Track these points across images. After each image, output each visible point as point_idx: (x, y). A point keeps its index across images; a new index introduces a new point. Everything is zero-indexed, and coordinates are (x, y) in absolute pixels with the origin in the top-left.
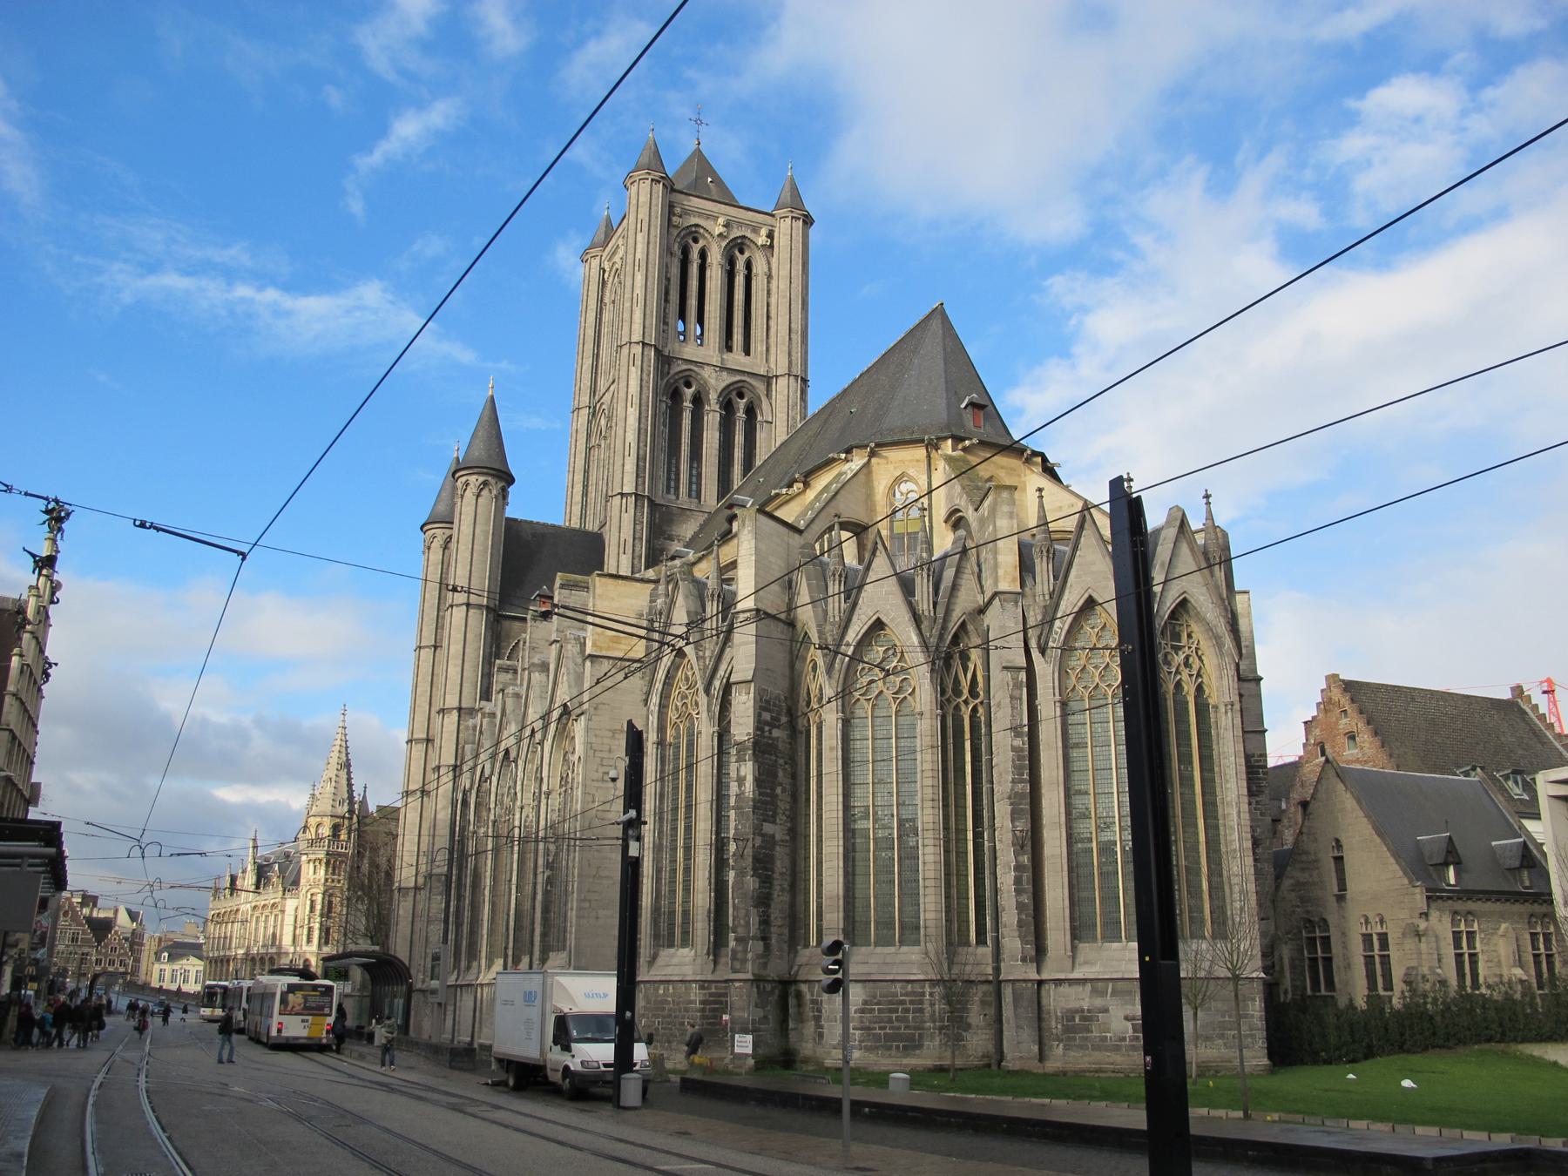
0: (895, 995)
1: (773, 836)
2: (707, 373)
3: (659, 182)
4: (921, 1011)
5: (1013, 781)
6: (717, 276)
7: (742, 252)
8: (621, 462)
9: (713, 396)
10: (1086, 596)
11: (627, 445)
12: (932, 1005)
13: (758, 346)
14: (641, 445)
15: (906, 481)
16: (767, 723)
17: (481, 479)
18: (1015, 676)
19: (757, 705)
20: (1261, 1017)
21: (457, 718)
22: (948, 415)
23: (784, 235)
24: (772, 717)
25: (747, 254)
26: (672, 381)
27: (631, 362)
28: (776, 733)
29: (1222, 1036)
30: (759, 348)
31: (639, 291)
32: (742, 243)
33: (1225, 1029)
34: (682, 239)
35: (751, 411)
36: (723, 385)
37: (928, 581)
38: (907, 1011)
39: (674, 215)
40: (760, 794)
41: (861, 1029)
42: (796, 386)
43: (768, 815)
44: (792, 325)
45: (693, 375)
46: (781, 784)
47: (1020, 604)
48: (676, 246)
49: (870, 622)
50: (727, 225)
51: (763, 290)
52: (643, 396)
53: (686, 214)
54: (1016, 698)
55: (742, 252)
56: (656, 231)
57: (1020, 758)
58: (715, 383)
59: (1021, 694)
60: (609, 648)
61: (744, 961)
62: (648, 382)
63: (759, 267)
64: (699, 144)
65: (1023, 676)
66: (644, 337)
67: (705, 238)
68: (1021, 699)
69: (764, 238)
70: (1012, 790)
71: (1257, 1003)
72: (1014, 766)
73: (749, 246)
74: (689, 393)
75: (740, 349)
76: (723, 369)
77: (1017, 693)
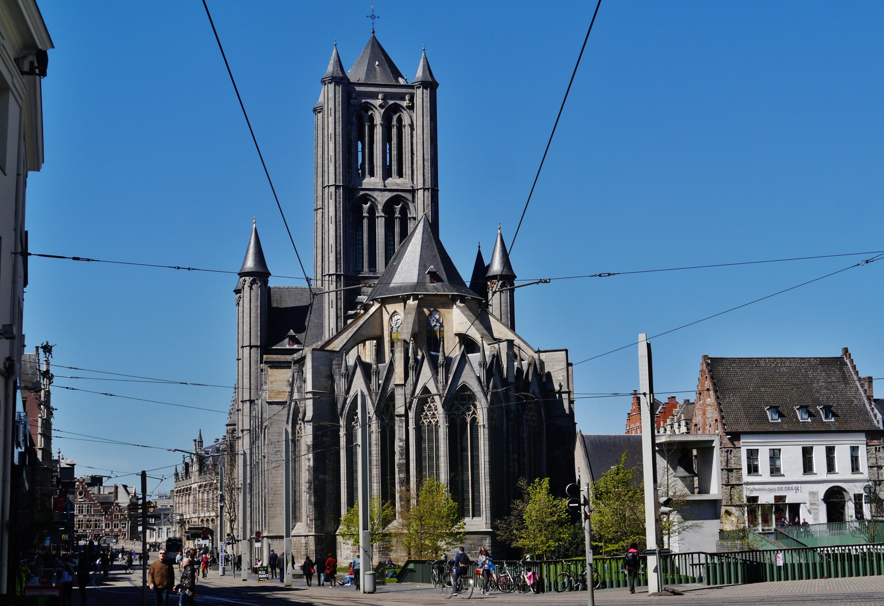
1: (324, 480)
2: (375, 194)
5: (399, 459)
6: (379, 132)
7: (395, 113)
8: (327, 256)
9: (380, 207)
11: (330, 246)
13: (407, 170)
14: (338, 245)
15: (397, 315)
20: (489, 546)
21: (249, 405)
22: (418, 281)
23: (419, 98)
27: (330, 198)
28: (324, 439)
30: (407, 173)
31: (332, 153)
33: (471, 550)
35: (404, 211)
36: (386, 199)
37: (376, 377)
39: (352, 99)
41: (353, 552)
42: (428, 194)
44: (425, 157)
48: (354, 118)
51: (408, 135)
52: (338, 216)
54: (401, 427)
56: (339, 114)
57: (402, 450)
60: (275, 398)
61: (312, 528)
62: (340, 208)
63: (406, 121)
64: (374, 32)
65: (403, 418)
67: (372, 109)
68: (402, 427)
69: (408, 101)
72: (400, 454)
74: (366, 207)
75: (396, 174)
77: (401, 425)
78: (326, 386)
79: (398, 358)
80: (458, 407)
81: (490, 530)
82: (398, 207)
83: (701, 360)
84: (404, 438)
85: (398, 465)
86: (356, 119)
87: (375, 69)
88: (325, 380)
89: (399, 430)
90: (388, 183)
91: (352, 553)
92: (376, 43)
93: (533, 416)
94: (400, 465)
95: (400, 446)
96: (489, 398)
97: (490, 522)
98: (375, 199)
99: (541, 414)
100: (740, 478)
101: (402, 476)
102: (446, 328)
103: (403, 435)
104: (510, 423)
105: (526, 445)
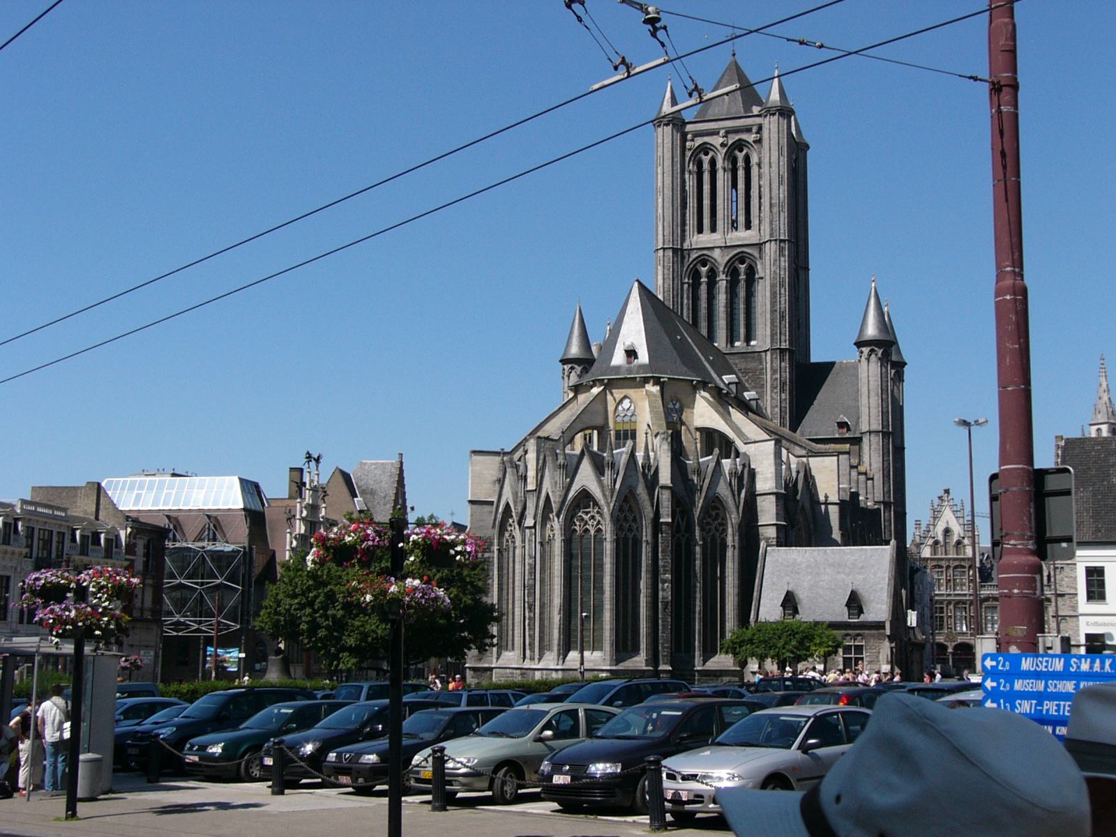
2: (716, 254)
7: (741, 151)
13: (755, 221)
17: (570, 366)
25: (744, 152)
26: (691, 266)
28: (486, 555)
35: (751, 271)
44: (773, 201)
45: (706, 257)
50: (725, 136)
58: (720, 258)
63: (754, 159)
64: (734, 55)
65: (533, 530)
66: (664, 244)
76: (726, 247)
81: (608, 668)
82: (742, 267)
83: (1053, 443)
86: (693, 164)
90: (731, 239)
92: (734, 67)
95: (529, 564)
96: (612, 505)
97: (609, 658)
98: (716, 260)
100: (1075, 608)
102: (639, 419)
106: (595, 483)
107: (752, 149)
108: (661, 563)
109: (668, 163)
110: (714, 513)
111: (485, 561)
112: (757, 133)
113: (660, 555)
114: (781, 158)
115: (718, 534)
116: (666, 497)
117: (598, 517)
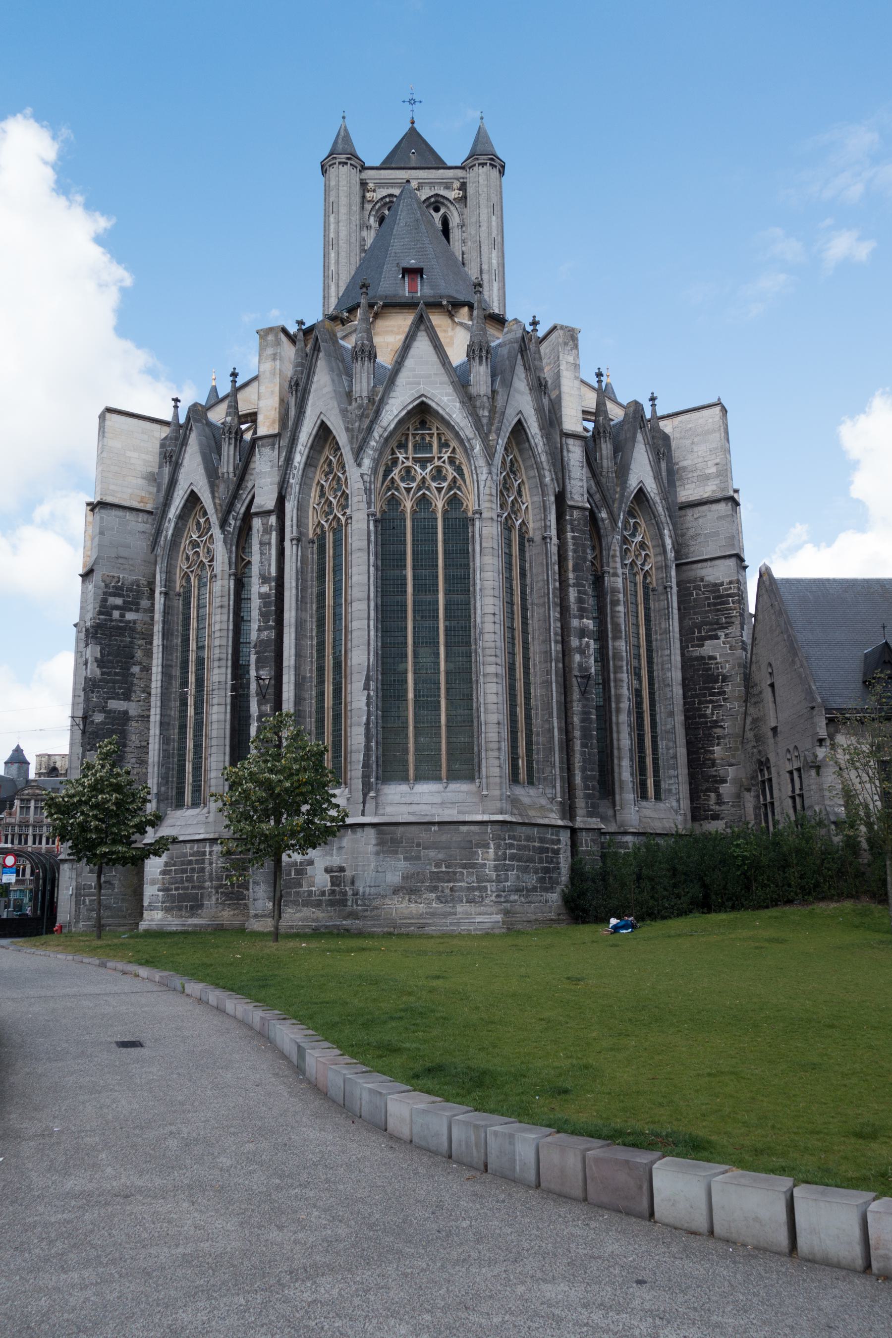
0: (185, 855)
1: (126, 712)
3: (346, 163)
4: (202, 870)
5: (260, 630)
7: (437, 210)
10: (319, 422)
12: (211, 864)
16: (117, 607)
18: (265, 521)
19: (100, 592)
24: (124, 602)
25: (442, 211)
28: (130, 616)
29: (434, 889)
32: (436, 202)
34: (377, 212)
37: (230, 444)
38: (193, 870)
39: (368, 191)
40: (103, 674)
43: (118, 694)
44: (485, 267)
46: (140, 663)
47: (277, 446)
48: (372, 219)
49: (186, 496)
53: (379, 188)
54: (265, 544)
55: (437, 210)
57: (266, 604)
59: (270, 539)
63: (454, 220)
64: (413, 123)
65: (273, 520)
68: (270, 544)
70: (258, 638)
71: (491, 851)
73: (443, 204)
78: (142, 497)
79: (268, 374)
80: (408, 470)
81: (500, 818)
84: (274, 573)
85: (255, 647)
86: (375, 221)
87: (409, 158)
88: (141, 482)
89: (262, 554)
91: (161, 893)
93: (642, 545)
94: (261, 645)
95: (262, 596)
99: (664, 546)
101: (265, 673)
103: (270, 565)
104: (569, 535)
105: (621, 608)
106: (450, 389)
107: (452, 208)
108: (573, 594)
109: (343, 210)
110: (632, 521)
111: (124, 629)
112: (459, 189)
113: (571, 575)
114: (494, 218)
115: (639, 563)
116: (575, 454)
117: (450, 472)
